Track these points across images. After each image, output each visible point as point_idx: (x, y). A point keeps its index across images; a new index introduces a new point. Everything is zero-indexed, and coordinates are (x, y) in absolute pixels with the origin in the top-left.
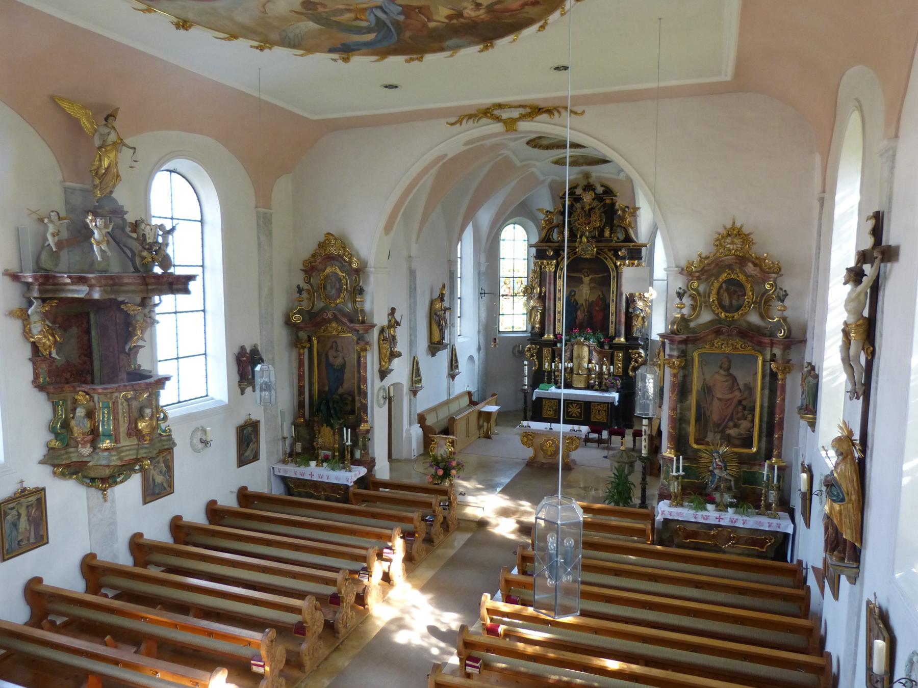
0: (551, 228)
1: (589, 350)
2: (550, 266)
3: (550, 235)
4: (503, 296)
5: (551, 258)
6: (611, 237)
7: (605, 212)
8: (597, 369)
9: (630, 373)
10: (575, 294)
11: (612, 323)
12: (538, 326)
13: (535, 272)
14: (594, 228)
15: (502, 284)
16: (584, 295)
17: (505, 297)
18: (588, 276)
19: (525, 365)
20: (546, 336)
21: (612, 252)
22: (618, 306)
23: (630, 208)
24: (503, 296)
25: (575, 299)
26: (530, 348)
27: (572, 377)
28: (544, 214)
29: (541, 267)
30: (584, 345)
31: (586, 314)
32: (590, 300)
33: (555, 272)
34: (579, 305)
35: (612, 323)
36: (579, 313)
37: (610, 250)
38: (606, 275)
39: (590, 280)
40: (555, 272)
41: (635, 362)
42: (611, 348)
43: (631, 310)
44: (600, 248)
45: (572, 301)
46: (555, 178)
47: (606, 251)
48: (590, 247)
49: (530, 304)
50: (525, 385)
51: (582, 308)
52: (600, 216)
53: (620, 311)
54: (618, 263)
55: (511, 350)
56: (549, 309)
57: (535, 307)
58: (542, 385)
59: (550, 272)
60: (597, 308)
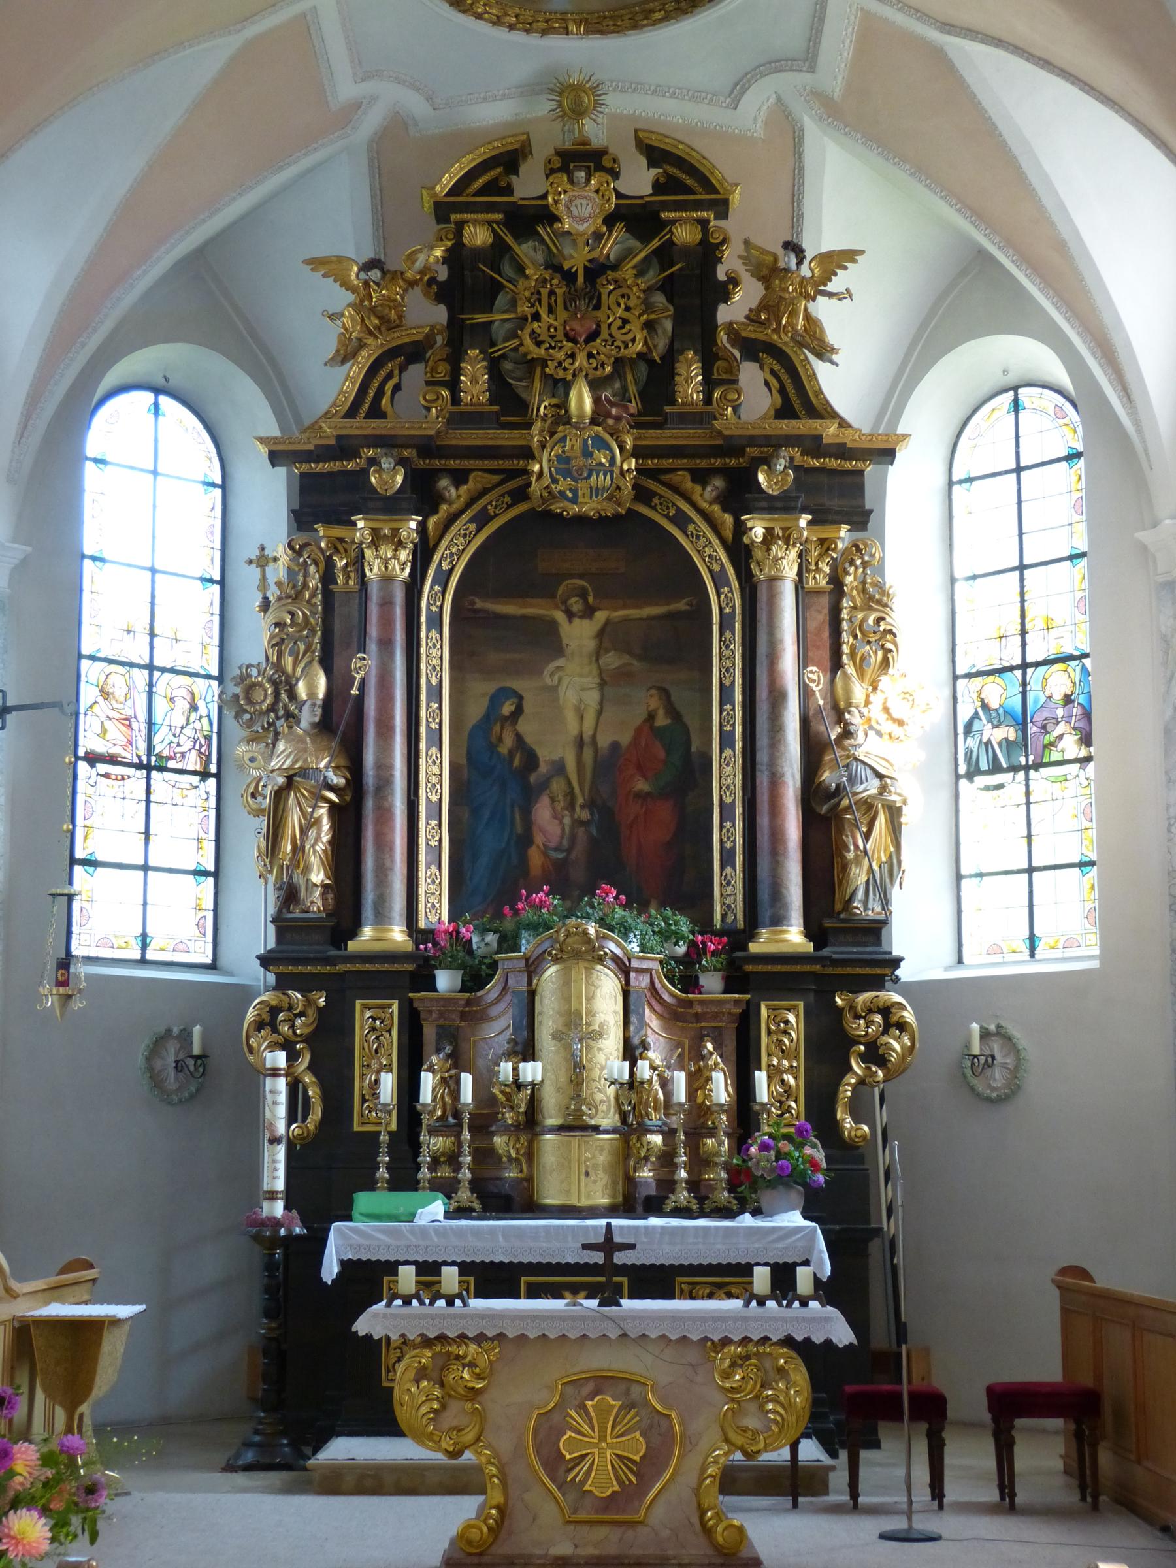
0: (390, 354)
1: (626, 994)
2: (387, 551)
3: (380, 392)
4: (93, 759)
5: (392, 506)
6: (708, 400)
7: (668, 287)
8: (681, 1094)
9: (848, 1123)
10: (519, 711)
11: (727, 858)
12: (318, 876)
13: (294, 593)
14: (619, 363)
15: (88, 694)
17: (102, 768)
18: (589, 612)
19: (275, 1072)
20: (367, 932)
21: (718, 483)
22: (762, 757)
23: (809, 254)
24: (93, 759)
25: (519, 738)
26: (274, 1011)
27: (531, 1155)
28: (346, 285)
29: (330, 564)
30: (601, 960)
31: (584, 815)
32: (604, 741)
33: (413, 589)
34: (543, 768)
35: (727, 858)
36: (542, 811)
37: (701, 477)
38: (681, 605)
39: (601, 634)
40: (413, 589)
41: (867, 1058)
42: (735, 980)
43: (827, 776)
45: (504, 750)
46: (415, 104)
47: (688, 484)
48: (605, 446)
49: (275, 763)
50: (272, 1196)
51: (558, 786)
52: (648, 307)
53: (776, 782)
54: (758, 532)
55: (140, 1060)
56: (384, 784)
57: (304, 772)
58: (364, 1201)
59: (387, 579)
60: (642, 785)
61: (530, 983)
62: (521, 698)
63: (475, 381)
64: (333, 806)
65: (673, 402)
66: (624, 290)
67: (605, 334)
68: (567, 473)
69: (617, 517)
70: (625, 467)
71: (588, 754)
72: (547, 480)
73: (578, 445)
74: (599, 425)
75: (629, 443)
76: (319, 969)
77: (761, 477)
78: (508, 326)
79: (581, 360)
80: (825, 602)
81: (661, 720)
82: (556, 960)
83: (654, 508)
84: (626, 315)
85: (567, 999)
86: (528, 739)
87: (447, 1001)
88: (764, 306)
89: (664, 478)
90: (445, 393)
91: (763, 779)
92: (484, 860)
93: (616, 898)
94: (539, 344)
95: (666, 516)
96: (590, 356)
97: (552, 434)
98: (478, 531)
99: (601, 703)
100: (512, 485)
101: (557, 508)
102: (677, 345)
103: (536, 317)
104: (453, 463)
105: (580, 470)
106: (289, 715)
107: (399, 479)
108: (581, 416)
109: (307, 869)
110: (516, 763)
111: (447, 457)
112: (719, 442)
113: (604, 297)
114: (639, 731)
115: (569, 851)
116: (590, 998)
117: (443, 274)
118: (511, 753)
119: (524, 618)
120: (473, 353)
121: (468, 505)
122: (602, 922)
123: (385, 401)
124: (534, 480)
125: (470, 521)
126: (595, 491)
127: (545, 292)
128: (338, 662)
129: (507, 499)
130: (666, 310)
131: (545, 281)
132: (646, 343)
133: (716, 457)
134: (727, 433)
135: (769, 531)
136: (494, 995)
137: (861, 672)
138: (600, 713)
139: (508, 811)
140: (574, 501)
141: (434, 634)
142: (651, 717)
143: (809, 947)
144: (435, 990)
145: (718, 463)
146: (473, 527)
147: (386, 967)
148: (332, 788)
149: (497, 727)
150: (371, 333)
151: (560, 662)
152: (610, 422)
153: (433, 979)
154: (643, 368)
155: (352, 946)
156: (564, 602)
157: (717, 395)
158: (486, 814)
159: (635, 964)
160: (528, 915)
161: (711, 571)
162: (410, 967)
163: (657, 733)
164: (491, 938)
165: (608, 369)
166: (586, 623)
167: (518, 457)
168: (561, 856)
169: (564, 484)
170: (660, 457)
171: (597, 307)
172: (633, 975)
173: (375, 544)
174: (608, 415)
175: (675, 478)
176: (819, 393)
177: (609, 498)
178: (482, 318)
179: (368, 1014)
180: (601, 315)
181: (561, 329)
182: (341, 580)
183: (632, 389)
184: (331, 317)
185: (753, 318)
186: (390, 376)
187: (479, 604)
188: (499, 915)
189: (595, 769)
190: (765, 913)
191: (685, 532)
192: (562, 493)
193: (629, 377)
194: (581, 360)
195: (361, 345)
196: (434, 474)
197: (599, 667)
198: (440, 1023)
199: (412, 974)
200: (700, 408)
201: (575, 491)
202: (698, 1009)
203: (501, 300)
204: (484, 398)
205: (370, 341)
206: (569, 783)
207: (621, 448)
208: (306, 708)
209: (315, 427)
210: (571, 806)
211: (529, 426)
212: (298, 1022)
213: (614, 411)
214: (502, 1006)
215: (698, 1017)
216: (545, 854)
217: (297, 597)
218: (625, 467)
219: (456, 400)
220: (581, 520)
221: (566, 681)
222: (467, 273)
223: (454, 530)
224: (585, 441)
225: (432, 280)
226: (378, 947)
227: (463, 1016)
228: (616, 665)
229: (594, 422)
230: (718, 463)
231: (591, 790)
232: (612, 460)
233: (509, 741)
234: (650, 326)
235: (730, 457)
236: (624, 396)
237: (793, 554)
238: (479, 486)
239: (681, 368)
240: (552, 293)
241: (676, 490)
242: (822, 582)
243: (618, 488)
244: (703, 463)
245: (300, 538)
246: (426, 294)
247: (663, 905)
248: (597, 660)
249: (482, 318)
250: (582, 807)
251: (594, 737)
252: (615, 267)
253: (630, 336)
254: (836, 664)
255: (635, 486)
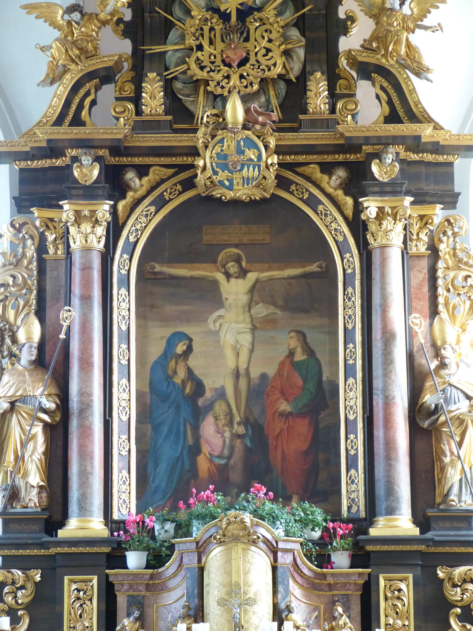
0: (89, 76)
1: (274, 569)
2: (86, 227)
3: (80, 107)
6: (333, 110)
10: (189, 350)
16: (229, 354)
18: (243, 273)
21: (341, 173)
22: (378, 383)
25: (190, 371)
28: (54, 24)
30: (254, 542)
31: (241, 430)
32: (255, 373)
34: (208, 394)
38: (314, 268)
39: (252, 290)
44: (289, 159)
45: (178, 380)
47: (318, 174)
48: (253, 145)
51: (220, 408)
52: (286, 39)
57: (24, 399)
59: (87, 250)
60: (284, 407)
61: (199, 561)
62: (191, 340)
63: (153, 97)
64: (46, 425)
65: (305, 112)
66: (268, 27)
67: (252, 60)
68: (225, 167)
69: (264, 200)
70: (270, 162)
71: (243, 383)
72: (209, 172)
73: (233, 145)
74: (249, 129)
75: (272, 143)
76: (36, 552)
77: (375, 168)
78: (178, 54)
79: (235, 80)
80: (424, 264)
81: (299, 356)
82: (220, 543)
83: (292, 193)
84: (269, 45)
85: (229, 574)
86: (197, 372)
87: (136, 576)
88: (375, 37)
89: (299, 170)
90: (131, 106)
91: (378, 401)
92: (163, 466)
93: (266, 494)
94: (202, 68)
95: (302, 199)
96: (242, 77)
97: (213, 137)
98: (157, 212)
99: (253, 344)
100: (183, 176)
101: (217, 193)
102: (308, 68)
103: (200, 48)
104: (137, 160)
105: (235, 164)
106: (12, 355)
107: (96, 173)
108: (235, 123)
109: (26, 475)
110: (188, 390)
111: (132, 156)
112: (342, 142)
113: (252, 32)
114: (282, 364)
115: (229, 458)
116: (246, 573)
117: (128, 15)
118: (184, 383)
119: (192, 278)
120: (152, 75)
121: (149, 192)
122: (255, 513)
123: (84, 113)
124: (199, 172)
125: (150, 204)
126: (247, 181)
127: (206, 28)
128: (50, 314)
129: (179, 187)
130: (300, 41)
131: (206, 20)
132: (284, 66)
133: (339, 153)
134: (347, 134)
135: (381, 209)
136: (171, 571)
137: (453, 317)
138: (252, 351)
139: (182, 428)
140: (230, 188)
141: (123, 291)
142: (292, 353)
143: (416, 531)
144: (125, 567)
145: (340, 158)
146: (153, 209)
147: (88, 549)
148: (45, 411)
149: (173, 363)
150: (73, 61)
151: (221, 312)
152: (258, 127)
153: (124, 558)
154: (282, 86)
155: (62, 533)
156: (224, 266)
157: (339, 105)
158: (165, 430)
159: (281, 545)
160: (198, 508)
161: (336, 241)
162: (107, 550)
163: (296, 366)
164: (170, 526)
165: (256, 87)
166: (240, 281)
167: (187, 155)
168: (223, 462)
169: (222, 175)
170: (296, 154)
171: (247, 39)
172: (279, 554)
173: (78, 222)
174: (256, 122)
175: (307, 170)
176: (418, 103)
177: (257, 186)
178: (158, 49)
179: (74, 586)
180: (249, 45)
181: (219, 57)
182: (51, 250)
183: (274, 102)
184: (42, 49)
185: (366, 47)
186: (88, 94)
187: (158, 268)
188: (175, 508)
189: (248, 396)
190: (381, 505)
191: (316, 212)
192: (221, 182)
193: (272, 93)
194: (235, 80)
195: (66, 70)
196: (122, 168)
197: (251, 316)
198: (131, 593)
199: (108, 556)
200: (327, 116)
201: (231, 181)
202: (330, 580)
203: (173, 35)
204: (161, 110)
205: (73, 67)
206: (229, 406)
207: (266, 147)
208: (25, 350)
209: (30, 133)
210: (230, 423)
211: (195, 131)
212: (19, 594)
213: (260, 119)
214: (178, 579)
215: (330, 587)
216: (211, 461)
217: (17, 264)
218: (270, 162)
219: (139, 112)
220: (236, 202)
221: (225, 327)
222: (146, 15)
223: (138, 211)
224: (239, 142)
225: (120, 21)
226: (81, 534)
227: (148, 587)
228: (265, 313)
229: (245, 127)
230: (340, 158)
231: (245, 411)
232: (259, 157)
233: (182, 374)
234: (287, 53)
235: (350, 153)
236: (268, 105)
237: (400, 226)
238: (158, 178)
239: (311, 85)
240: (212, 29)
241: (308, 179)
242: (423, 249)
243: (264, 178)
244: (329, 158)
245: (20, 219)
246: (115, 31)
247: (302, 500)
248: (249, 310)
249: (158, 49)
250: (239, 424)
251: (247, 369)
252: (260, 9)
253: (272, 61)
254: (434, 312)
255: (278, 177)
